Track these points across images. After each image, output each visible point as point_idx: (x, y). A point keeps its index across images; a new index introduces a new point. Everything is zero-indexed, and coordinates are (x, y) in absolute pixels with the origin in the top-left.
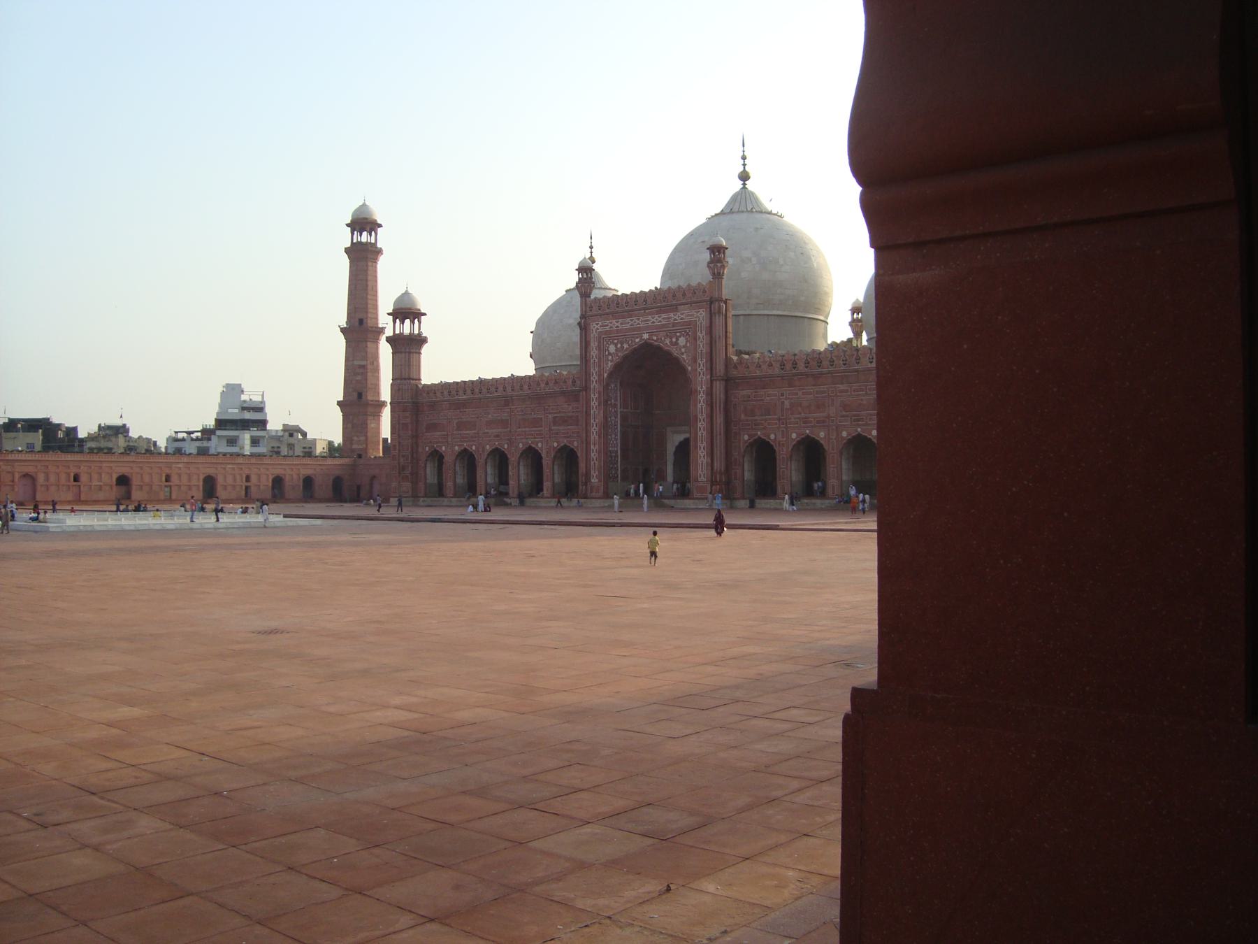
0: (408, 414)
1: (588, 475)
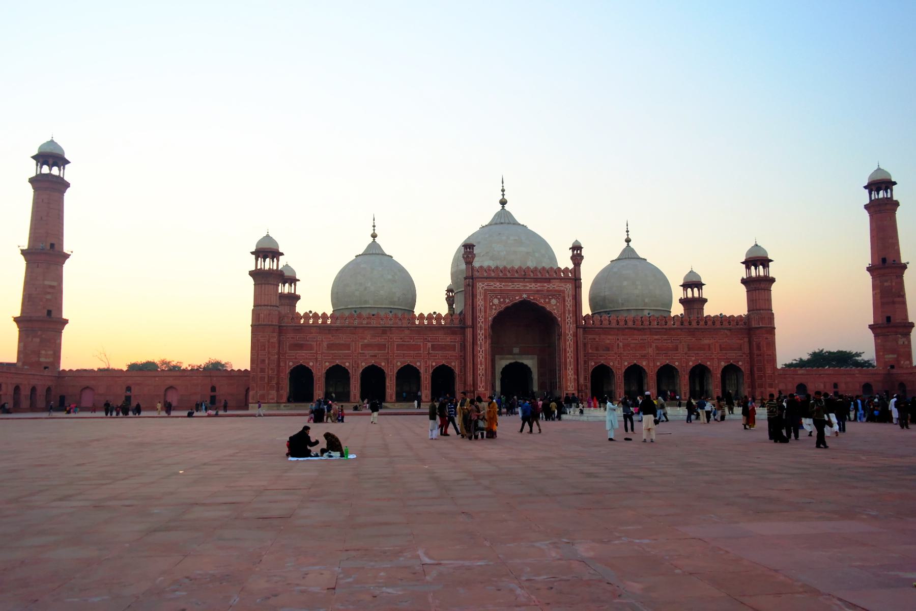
0: (275, 334)
1: (475, 385)
